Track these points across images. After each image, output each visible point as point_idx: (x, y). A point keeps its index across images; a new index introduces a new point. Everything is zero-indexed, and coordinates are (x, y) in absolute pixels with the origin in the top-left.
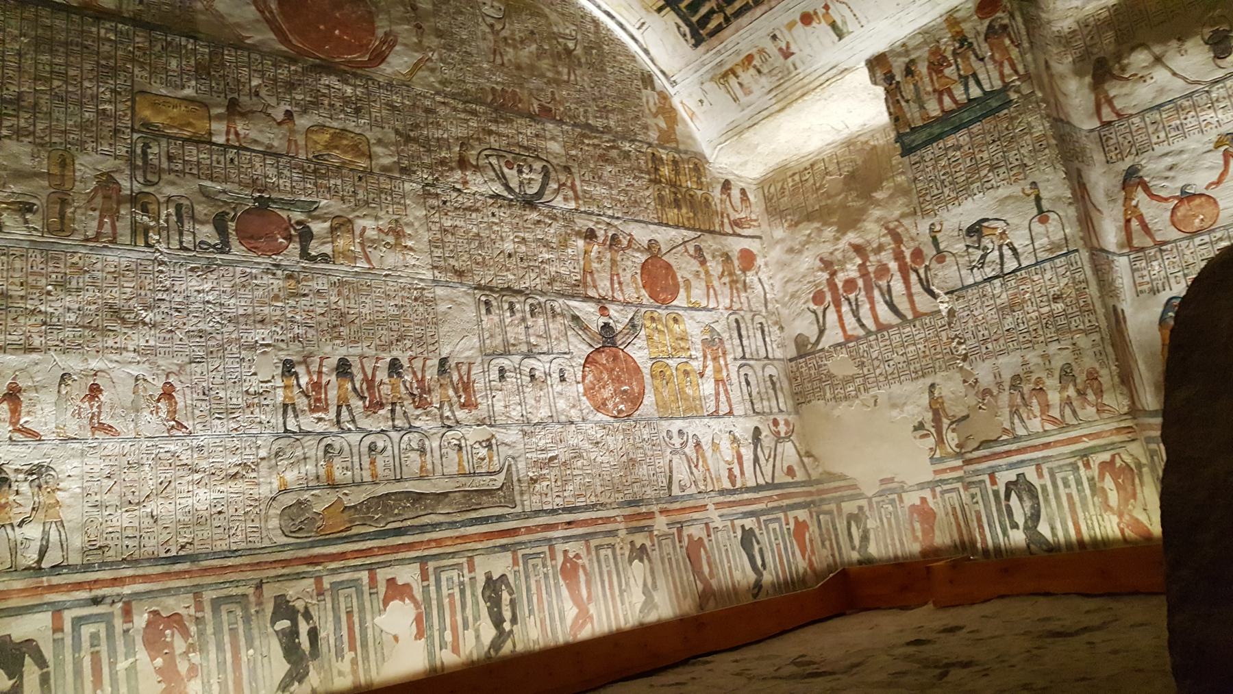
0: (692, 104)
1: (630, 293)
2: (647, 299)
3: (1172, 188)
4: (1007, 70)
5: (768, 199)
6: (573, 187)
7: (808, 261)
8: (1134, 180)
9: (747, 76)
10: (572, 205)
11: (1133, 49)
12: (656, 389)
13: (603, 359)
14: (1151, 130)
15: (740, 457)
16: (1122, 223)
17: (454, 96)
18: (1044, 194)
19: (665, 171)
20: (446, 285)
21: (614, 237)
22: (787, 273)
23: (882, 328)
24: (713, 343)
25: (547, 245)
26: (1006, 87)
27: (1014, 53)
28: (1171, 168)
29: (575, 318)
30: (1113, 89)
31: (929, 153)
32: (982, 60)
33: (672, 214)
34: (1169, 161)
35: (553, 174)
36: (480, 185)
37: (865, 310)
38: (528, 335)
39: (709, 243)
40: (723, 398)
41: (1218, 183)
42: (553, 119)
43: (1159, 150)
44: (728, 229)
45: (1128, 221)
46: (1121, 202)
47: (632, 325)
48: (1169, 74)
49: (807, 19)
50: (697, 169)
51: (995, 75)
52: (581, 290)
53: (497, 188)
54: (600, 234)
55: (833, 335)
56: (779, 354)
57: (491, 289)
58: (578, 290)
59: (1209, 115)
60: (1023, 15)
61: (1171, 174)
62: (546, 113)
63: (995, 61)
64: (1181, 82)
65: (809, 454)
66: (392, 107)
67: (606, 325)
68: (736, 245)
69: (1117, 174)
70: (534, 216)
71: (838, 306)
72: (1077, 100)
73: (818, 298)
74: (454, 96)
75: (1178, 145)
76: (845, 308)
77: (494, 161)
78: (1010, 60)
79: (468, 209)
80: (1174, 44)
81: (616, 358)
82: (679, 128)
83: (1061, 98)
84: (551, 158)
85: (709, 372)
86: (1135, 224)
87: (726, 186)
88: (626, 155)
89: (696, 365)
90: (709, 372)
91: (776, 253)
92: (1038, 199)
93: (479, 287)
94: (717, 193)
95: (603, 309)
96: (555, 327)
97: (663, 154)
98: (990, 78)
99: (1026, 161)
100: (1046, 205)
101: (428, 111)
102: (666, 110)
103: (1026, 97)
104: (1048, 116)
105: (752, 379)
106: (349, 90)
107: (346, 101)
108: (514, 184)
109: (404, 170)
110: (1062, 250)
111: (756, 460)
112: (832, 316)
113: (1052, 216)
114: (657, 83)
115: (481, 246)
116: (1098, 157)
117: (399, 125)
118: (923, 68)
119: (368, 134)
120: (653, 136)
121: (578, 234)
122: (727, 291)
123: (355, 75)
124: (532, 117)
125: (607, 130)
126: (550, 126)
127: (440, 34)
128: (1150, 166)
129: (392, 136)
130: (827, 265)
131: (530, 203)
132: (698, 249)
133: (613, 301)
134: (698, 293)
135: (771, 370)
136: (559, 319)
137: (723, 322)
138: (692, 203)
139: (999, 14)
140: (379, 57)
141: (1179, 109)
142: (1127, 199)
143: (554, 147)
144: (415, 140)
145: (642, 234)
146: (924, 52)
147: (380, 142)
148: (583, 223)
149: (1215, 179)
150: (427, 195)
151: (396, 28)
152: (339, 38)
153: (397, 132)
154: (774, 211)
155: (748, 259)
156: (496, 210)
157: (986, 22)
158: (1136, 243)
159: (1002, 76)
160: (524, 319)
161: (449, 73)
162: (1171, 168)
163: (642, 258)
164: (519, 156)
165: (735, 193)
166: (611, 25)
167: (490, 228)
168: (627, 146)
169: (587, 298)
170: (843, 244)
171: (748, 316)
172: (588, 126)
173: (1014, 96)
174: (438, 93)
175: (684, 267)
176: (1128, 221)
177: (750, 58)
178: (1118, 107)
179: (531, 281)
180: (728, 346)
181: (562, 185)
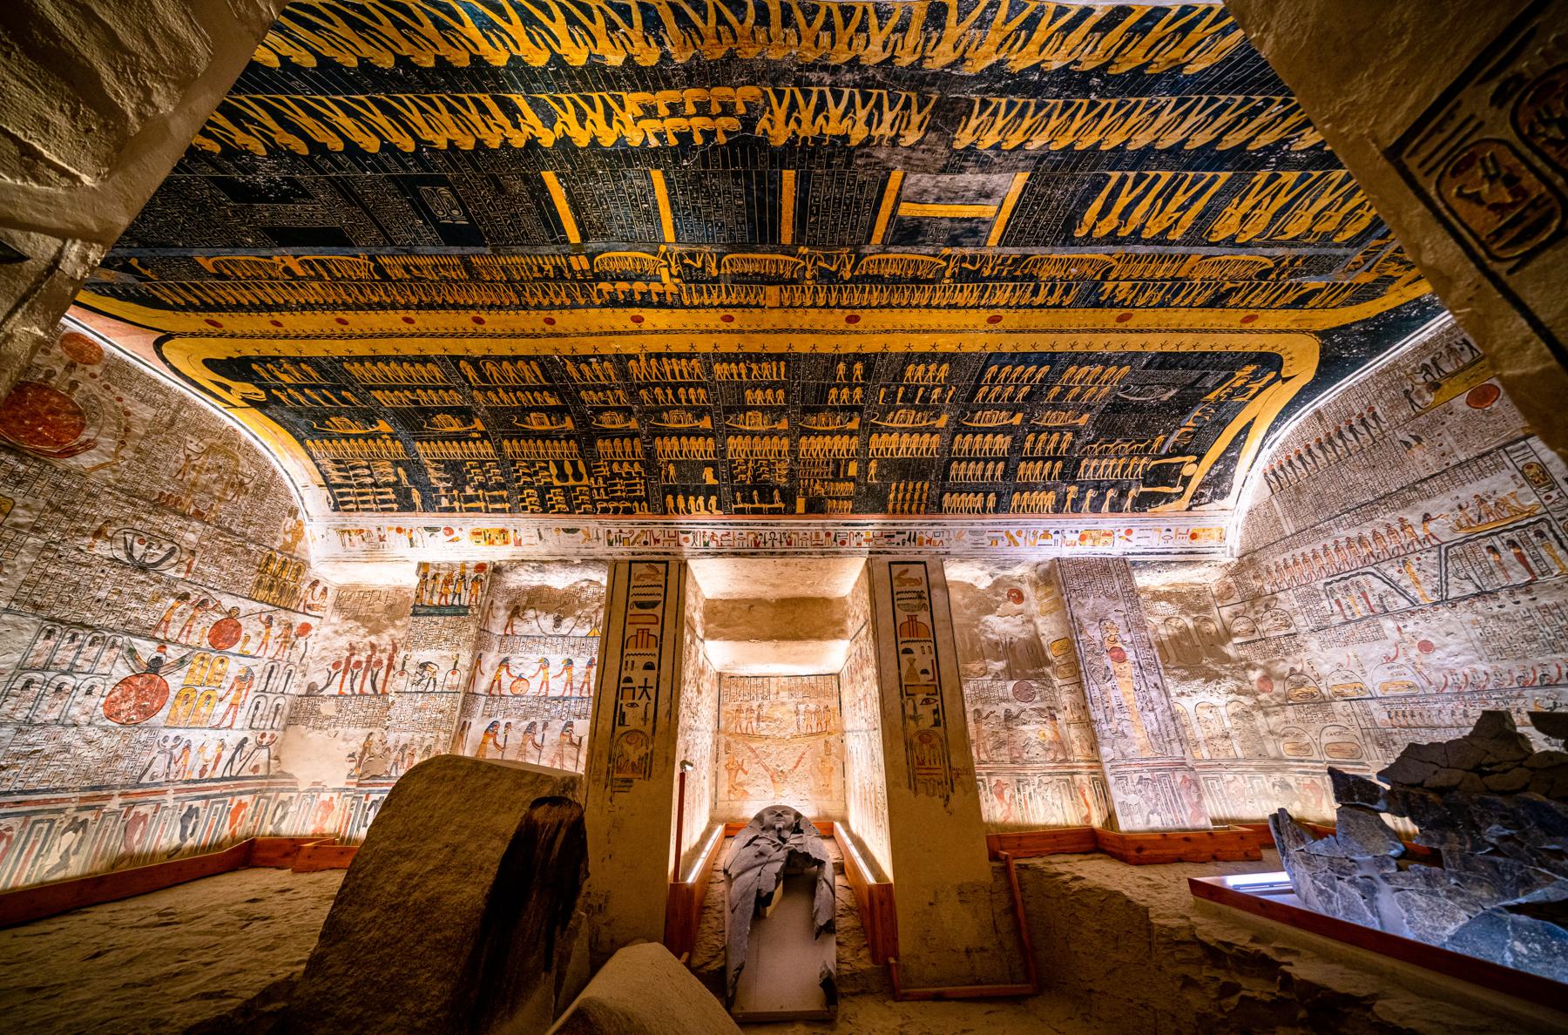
0: (318, 536)
1: (194, 639)
2: (206, 643)
5: (339, 598)
6: (189, 566)
7: (343, 642)
9: (355, 538)
10: (182, 575)
12: (174, 706)
13: (138, 682)
15: (219, 757)
17: (122, 491)
19: (273, 567)
20: (18, 613)
21: (204, 603)
22: (326, 644)
23: (362, 693)
24: (245, 679)
25: (140, 598)
29: (132, 651)
30: (516, 621)
31: (423, 620)
33: (262, 593)
35: (178, 554)
36: (103, 549)
37: (358, 682)
38: (76, 657)
39: (283, 615)
40: (229, 717)
42: (202, 521)
44: (301, 609)
47: (182, 661)
49: (399, 530)
50: (299, 570)
52: (150, 633)
53: (121, 555)
54: (193, 598)
55: (333, 689)
56: (293, 691)
57: (62, 622)
58: (147, 633)
62: (199, 515)
65: (277, 758)
66: (57, 486)
67: (158, 659)
68: (299, 619)
70: (142, 578)
71: (345, 673)
73: (336, 665)
74: (122, 491)
76: (349, 676)
77: (129, 537)
79: (82, 565)
81: (151, 681)
82: (300, 544)
84: (183, 544)
85: (229, 699)
87: (315, 583)
88: (249, 552)
89: (220, 693)
90: (229, 699)
91: (327, 630)
93: (52, 619)
94: (305, 586)
95: (162, 648)
96: (107, 655)
97: (279, 556)
98: (465, 601)
101: (90, 495)
102: (298, 533)
105: (261, 706)
106: (22, 467)
107: (13, 473)
108: (137, 555)
109: (36, 530)
110: (454, 690)
111: (232, 760)
112: (339, 678)
114: (300, 517)
115: (75, 590)
117: (54, 500)
118: (441, 579)
119: (18, 500)
120: (277, 545)
121: (173, 595)
122: (276, 647)
123: (36, 459)
124: (184, 515)
125: (243, 534)
126: (196, 524)
127: (138, 450)
129: (42, 504)
130: (352, 649)
131: (143, 568)
132: (270, 618)
133: (176, 642)
134: (251, 647)
135: (281, 701)
136: (116, 650)
137: (261, 667)
138: (282, 590)
140: (71, 453)
143: (192, 537)
144: (64, 512)
145: (228, 602)
146: (445, 573)
147: (26, 507)
148: (181, 588)
150: (47, 547)
151: (100, 438)
152: (40, 433)
153: (49, 503)
154: (339, 606)
155: (306, 628)
156: (107, 569)
160: (80, 647)
161: (129, 476)
163: (220, 617)
164: (149, 539)
165: (319, 589)
166: (285, 476)
167: (93, 578)
168: (252, 547)
169: (153, 638)
170: (366, 640)
171: (283, 665)
172: (229, 530)
174: (109, 486)
175: (251, 627)
177: (361, 531)
179: (110, 621)
180: (256, 682)
181: (180, 561)
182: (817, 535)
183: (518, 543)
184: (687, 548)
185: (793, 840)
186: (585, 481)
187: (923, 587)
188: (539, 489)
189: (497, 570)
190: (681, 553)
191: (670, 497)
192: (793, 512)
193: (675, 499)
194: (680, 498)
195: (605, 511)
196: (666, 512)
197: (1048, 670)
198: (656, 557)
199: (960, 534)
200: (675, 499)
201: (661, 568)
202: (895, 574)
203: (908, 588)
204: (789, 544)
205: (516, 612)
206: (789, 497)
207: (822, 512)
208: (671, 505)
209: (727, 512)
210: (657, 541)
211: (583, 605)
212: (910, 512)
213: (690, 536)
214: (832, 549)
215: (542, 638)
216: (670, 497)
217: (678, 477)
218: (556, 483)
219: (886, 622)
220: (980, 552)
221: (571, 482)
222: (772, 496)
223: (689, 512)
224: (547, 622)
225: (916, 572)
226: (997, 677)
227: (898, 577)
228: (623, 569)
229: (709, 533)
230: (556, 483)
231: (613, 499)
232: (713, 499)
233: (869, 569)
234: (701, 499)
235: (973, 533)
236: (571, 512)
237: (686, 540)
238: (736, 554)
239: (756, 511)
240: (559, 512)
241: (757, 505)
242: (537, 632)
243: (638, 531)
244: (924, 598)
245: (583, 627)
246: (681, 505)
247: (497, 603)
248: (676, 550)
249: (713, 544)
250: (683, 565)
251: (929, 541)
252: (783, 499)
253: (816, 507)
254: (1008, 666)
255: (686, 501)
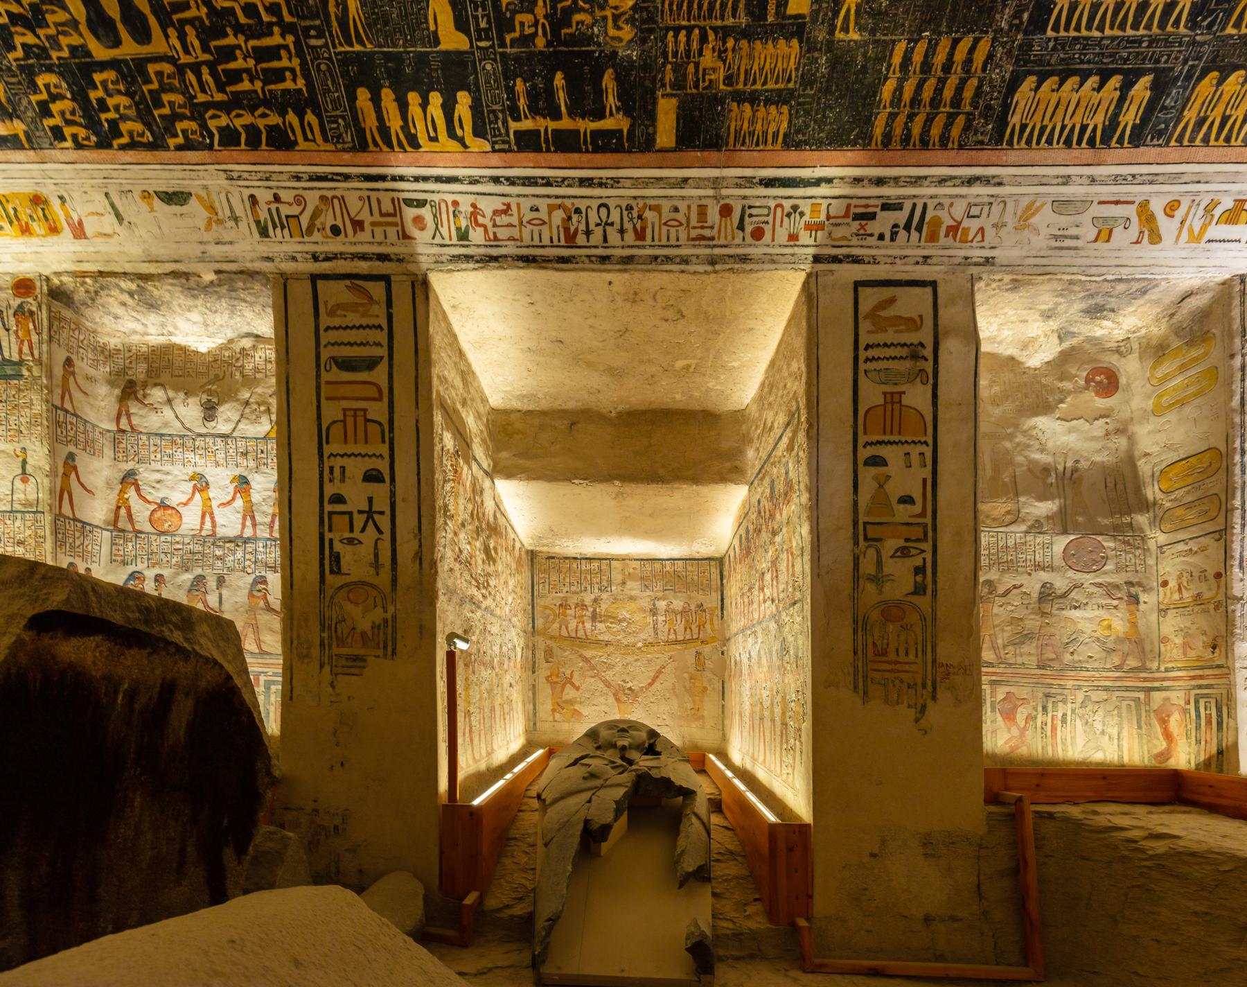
3: (155, 496)
4: (26, 349)
8: (130, 480)
11: (156, 385)
14: (152, 449)
16: (114, 507)
18: (29, 460)
26: (21, 363)
27: (35, 338)
28: (159, 482)
30: (134, 408)
32: (8, 330)
34: (158, 476)
41: (185, 504)
43: (157, 466)
45: (119, 508)
46: (117, 491)
48: (173, 415)
51: (15, 348)
59: (190, 455)
60: (49, 310)
61: (158, 486)
63: (17, 336)
64: (179, 424)
69: (120, 470)
72: (103, 404)
75: (167, 468)
78: (30, 342)
80: (182, 395)
83: (77, 394)
86: (123, 511)
92: (24, 462)
99: (22, 428)
100: (29, 469)
103: (34, 378)
104: (47, 401)
113: (32, 479)
116: (108, 452)
128: (145, 474)
139: (30, 300)
141: (174, 443)
142: (122, 491)
149: (184, 501)
157: (18, 301)
158: (120, 525)
159: (20, 351)
162: (159, 482)
173: (25, 373)
176: (119, 508)
178: (134, 422)
182: (702, 211)
183: (79, 232)
184: (424, 246)
185: (644, 763)
186: (158, 45)
187: (926, 336)
188: (63, 69)
189: (58, 295)
190: (412, 258)
191: (363, 95)
192: (648, 145)
193: (376, 100)
194: (388, 98)
195: (229, 138)
196: (361, 145)
197: (1141, 519)
198: (363, 267)
199: (1031, 210)
200: (376, 100)
201: (377, 290)
202: (864, 308)
203: (890, 336)
204: (640, 235)
205: (130, 391)
206: (639, 105)
207: (715, 143)
208: (371, 122)
209: (501, 146)
210: (358, 225)
211: (250, 381)
212: (925, 143)
213: (426, 212)
214: (728, 247)
215: (183, 440)
216: (363, 95)
217: (370, 25)
218: (100, 52)
219: (838, 403)
220: (1067, 258)
221: (129, 48)
222: (599, 93)
223: (414, 143)
224: (190, 411)
225: (913, 303)
226: (1037, 527)
227: (872, 315)
228: (301, 291)
229: (465, 208)
230: (100, 52)
231: (235, 103)
232: (464, 100)
233: (810, 294)
234: (436, 99)
235: (1061, 205)
236: (156, 145)
237: (418, 221)
238: (528, 261)
239: (566, 143)
240: (133, 145)
241: (565, 123)
242: (176, 428)
243: (312, 199)
244: (924, 359)
245: (256, 421)
246: (395, 124)
247: (83, 366)
248: (398, 249)
249: (477, 236)
250: (421, 287)
251: (953, 230)
252: (626, 108)
253: (702, 131)
254: (1062, 512)
255: (403, 106)
